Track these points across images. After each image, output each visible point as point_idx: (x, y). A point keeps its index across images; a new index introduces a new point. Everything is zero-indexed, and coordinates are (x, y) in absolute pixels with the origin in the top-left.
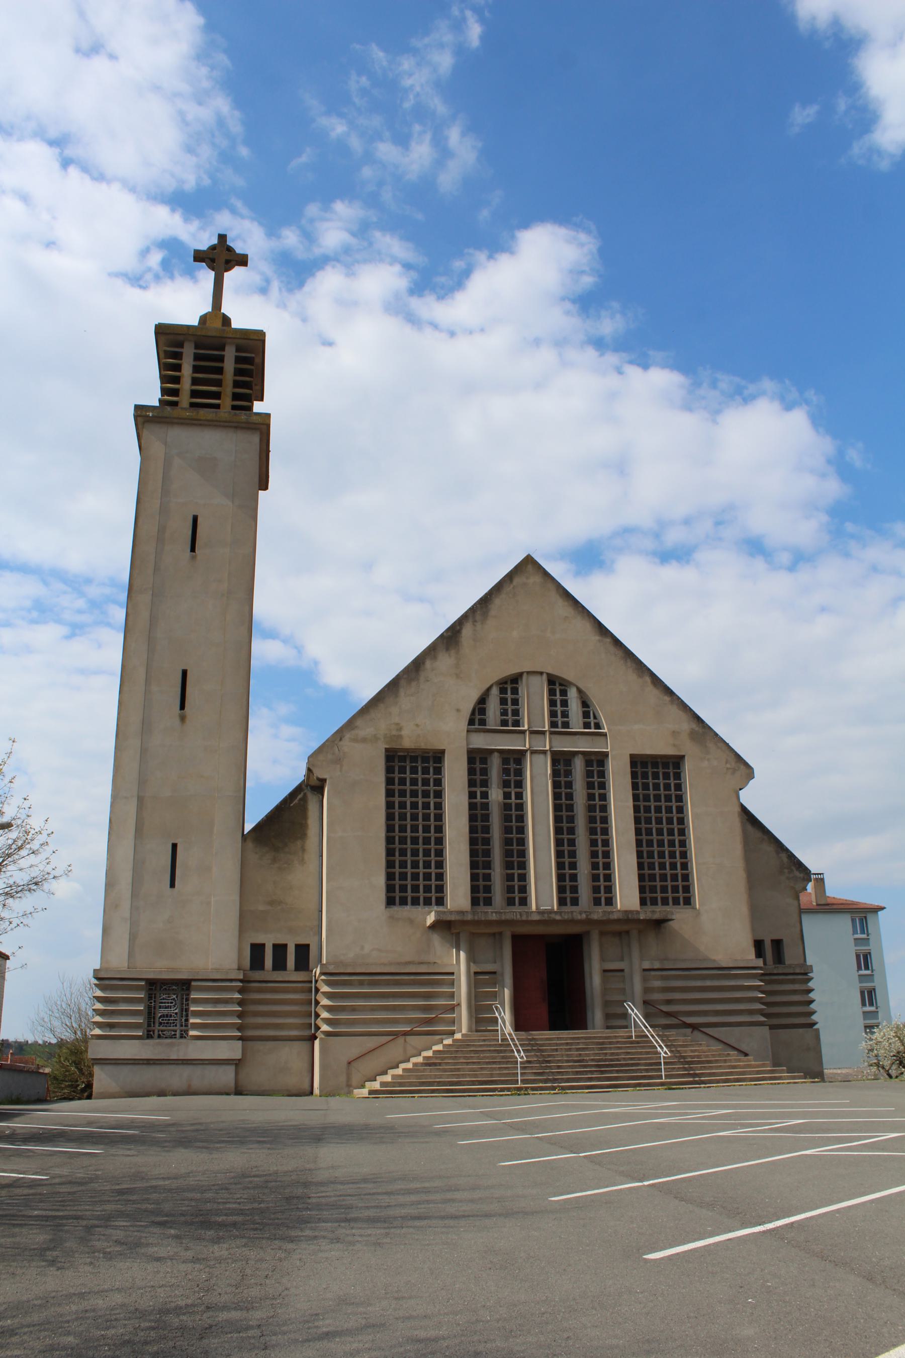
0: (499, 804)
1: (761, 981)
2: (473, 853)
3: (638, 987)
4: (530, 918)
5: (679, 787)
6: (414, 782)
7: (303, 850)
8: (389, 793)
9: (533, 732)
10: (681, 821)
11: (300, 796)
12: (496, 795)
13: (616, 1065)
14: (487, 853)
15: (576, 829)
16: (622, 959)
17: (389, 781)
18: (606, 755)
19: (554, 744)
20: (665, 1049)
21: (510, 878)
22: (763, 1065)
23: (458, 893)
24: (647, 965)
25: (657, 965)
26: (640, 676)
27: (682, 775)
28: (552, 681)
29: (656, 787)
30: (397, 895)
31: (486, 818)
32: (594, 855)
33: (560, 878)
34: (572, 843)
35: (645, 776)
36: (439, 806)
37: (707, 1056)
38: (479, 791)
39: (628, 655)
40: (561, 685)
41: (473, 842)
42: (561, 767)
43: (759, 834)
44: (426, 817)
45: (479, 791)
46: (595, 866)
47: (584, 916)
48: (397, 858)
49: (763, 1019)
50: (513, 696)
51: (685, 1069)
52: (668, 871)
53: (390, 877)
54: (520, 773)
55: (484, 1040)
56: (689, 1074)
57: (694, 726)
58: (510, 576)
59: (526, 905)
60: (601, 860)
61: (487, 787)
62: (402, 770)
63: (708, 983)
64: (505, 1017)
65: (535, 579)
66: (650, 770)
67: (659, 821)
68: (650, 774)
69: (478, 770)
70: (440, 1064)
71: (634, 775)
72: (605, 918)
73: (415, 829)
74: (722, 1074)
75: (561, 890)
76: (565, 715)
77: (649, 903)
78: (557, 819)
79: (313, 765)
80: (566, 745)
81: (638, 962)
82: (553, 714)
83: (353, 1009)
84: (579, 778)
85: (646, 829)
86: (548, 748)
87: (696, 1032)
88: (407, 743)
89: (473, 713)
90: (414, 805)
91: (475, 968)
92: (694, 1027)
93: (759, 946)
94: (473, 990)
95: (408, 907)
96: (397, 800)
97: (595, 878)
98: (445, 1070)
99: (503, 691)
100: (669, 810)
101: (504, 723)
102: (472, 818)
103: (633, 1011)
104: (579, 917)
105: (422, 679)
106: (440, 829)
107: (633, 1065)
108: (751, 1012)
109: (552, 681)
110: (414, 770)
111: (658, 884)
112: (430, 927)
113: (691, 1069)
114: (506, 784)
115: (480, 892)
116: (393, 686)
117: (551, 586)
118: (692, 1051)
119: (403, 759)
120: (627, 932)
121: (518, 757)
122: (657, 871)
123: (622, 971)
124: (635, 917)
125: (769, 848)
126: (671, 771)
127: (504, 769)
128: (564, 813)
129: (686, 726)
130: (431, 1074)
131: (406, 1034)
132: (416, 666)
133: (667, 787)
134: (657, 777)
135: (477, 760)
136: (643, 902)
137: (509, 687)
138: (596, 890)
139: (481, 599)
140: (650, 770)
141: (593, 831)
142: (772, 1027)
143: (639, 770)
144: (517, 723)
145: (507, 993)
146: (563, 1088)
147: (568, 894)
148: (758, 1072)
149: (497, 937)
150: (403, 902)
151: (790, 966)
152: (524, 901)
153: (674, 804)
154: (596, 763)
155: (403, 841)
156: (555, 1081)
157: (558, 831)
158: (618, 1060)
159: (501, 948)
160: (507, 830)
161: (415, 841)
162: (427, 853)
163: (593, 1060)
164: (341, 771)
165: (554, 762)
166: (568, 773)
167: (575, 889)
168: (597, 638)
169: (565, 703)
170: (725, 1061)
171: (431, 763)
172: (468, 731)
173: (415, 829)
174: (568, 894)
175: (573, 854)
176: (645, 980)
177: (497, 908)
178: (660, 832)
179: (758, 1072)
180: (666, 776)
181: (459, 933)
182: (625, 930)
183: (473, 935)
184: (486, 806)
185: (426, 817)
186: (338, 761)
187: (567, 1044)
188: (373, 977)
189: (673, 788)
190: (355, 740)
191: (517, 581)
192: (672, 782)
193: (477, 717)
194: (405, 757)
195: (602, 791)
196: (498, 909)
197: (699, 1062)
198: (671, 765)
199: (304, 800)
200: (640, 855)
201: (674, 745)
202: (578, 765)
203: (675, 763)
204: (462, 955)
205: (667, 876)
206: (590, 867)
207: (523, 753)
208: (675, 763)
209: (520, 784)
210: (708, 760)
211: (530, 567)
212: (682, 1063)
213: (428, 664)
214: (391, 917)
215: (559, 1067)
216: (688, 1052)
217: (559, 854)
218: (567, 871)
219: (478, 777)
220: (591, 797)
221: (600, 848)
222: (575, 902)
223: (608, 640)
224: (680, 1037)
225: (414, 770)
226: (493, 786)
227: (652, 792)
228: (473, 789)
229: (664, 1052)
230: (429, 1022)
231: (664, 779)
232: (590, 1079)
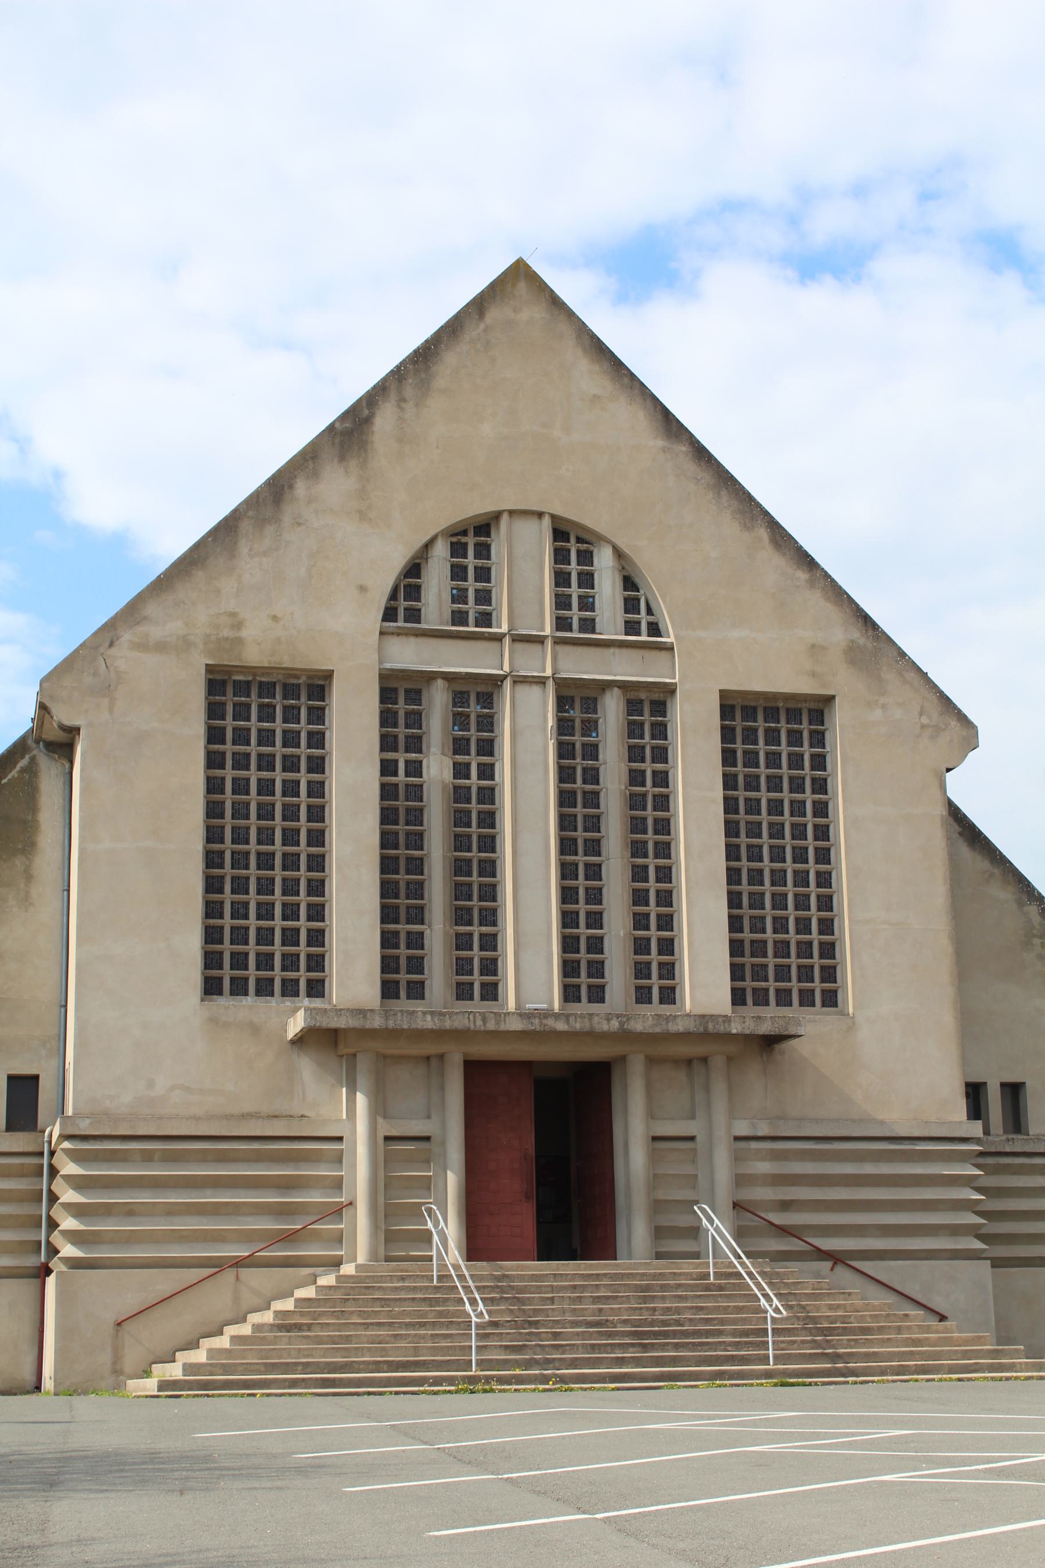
0: (444, 787)
1: (978, 1166)
2: (387, 889)
3: (723, 1168)
4: (503, 1027)
5: (819, 762)
6: (266, 738)
7: (28, 876)
8: (214, 761)
9: (519, 639)
10: (823, 833)
11: (23, 763)
12: (437, 768)
13: (674, 1334)
14: (417, 890)
15: (603, 843)
16: (692, 1117)
17: (214, 735)
18: (670, 690)
19: (562, 665)
20: (776, 1301)
21: (463, 942)
22: (978, 1340)
23: (353, 971)
24: (742, 1128)
25: (764, 1130)
26: (747, 528)
27: (827, 735)
28: (562, 532)
29: (773, 760)
30: (227, 973)
31: (416, 816)
32: (639, 897)
33: (569, 944)
34: (594, 872)
35: (750, 736)
36: (318, 790)
37: (862, 1319)
38: (401, 758)
39: (725, 480)
40: (579, 540)
41: (387, 865)
42: (576, 714)
43: (985, 865)
44: (291, 813)
45: (401, 758)
46: (640, 921)
47: (615, 1024)
48: (228, 897)
49: (979, 1245)
50: (480, 562)
51: (816, 1344)
52: (792, 936)
53: (212, 935)
54: (488, 723)
55: (403, 1279)
56: (825, 1356)
57: (856, 633)
58: (479, 305)
59: (496, 999)
60: (653, 909)
61: (420, 751)
62: (242, 712)
63: (869, 1169)
64: (447, 1229)
65: (533, 313)
66: (761, 725)
67: (777, 831)
68: (761, 734)
69: (401, 715)
70: (309, 1327)
71: (727, 734)
72: (658, 1030)
73: (266, 836)
74: (891, 1356)
75: (569, 969)
76: (587, 604)
77: (749, 1000)
78: (565, 822)
79: (52, 697)
80: (584, 666)
82: (562, 602)
83: (130, 1211)
84: (611, 734)
85: (749, 847)
86: (549, 672)
87: (840, 1269)
88: (254, 656)
89: (394, 596)
90: (266, 787)
91: (386, 1128)
92: (836, 1258)
93: (975, 1093)
94: (381, 1173)
95: (250, 1000)
96: (229, 774)
97: (641, 946)
98: (319, 1340)
99: (458, 550)
100: (798, 808)
101: (459, 618)
102: (387, 816)
104: (605, 1027)
105: (287, 519)
106: (318, 838)
107: (708, 1333)
108: (955, 1230)
109: (562, 532)
110: (267, 713)
111: (771, 961)
112: (293, 1042)
114: (460, 746)
115: (400, 970)
116: (226, 531)
117: (564, 327)
118: (831, 1307)
119: (242, 688)
120: (705, 1060)
121: (486, 690)
122: (769, 935)
123: (692, 1139)
124: (722, 1029)
125: (1004, 894)
126: (805, 727)
127: (456, 715)
128: (579, 810)
129: (840, 633)
130: (290, 1348)
131: (238, 1263)
132: (277, 490)
133: (796, 761)
134: (777, 741)
135: (400, 697)
137: (471, 541)
138: (641, 971)
139: (416, 352)
140: (761, 725)
141: (637, 849)
142: (997, 1263)
143: (739, 723)
144: (485, 619)
145: (453, 1182)
146: (563, 1380)
147: (583, 980)
148: (965, 1355)
149: (432, 1063)
150: (239, 988)
151: (1038, 1138)
152: (491, 992)
153: (809, 797)
154: (650, 706)
155: (240, 860)
156: (547, 1363)
157: (566, 846)
158: (678, 1323)
159: (442, 1088)
160: (460, 842)
161: (266, 861)
162: (291, 887)
163: (625, 1322)
164: (111, 711)
165: (563, 702)
166: (590, 726)
167: (597, 969)
168: (660, 443)
169: (587, 580)
170: (899, 1330)
171: (303, 698)
172: (381, 633)
173: (266, 836)
174: (583, 980)
175: (595, 896)
176: (737, 1158)
177: (437, 1004)
178: (777, 854)
179: (965, 1355)
180: (795, 738)
181: (355, 1055)
182: (697, 1054)
183: (384, 1059)
184: (416, 792)
185: (291, 813)
186: (107, 690)
187: (575, 1287)
188: (171, 1144)
189: (807, 763)
190: (143, 646)
191: (494, 314)
192: (807, 750)
193: (402, 604)
194: (248, 683)
195: (659, 766)
196: (437, 1004)
197: (845, 1331)
198: (806, 716)
199: (32, 770)
200: (734, 900)
201: (814, 674)
202: (612, 712)
203: (812, 712)
204: (361, 1100)
205: (789, 948)
206: (629, 922)
207: (496, 681)
208: (812, 712)
209: (487, 747)
210: (884, 707)
211: (522, 286)
213: (301, 487)
214: (213, 1020)
215: (556, 1336)
216: (822, 1310)
217: (567, 895)
218: (583, 931)
219: (401, 731)
220: (636, 778)
221: (652, 885)
222: (597, 994)
223: (684, 448)
224: (807, 1275)
225: (267, 713)
226: (433, 749)
227: (763, 771)
228: (391, 755)
229: (773, 1308)
230: (288, 1238)
231: (790, 744)
232: (621, 1362)
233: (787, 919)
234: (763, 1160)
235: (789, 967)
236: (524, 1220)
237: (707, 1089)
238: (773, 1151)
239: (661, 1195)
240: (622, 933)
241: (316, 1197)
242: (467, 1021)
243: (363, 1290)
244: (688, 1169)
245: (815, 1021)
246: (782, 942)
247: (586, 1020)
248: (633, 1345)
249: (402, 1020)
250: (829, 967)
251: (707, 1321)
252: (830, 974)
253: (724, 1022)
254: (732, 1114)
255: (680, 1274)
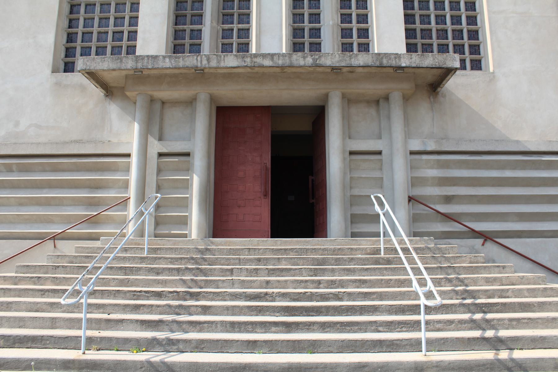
3: (399, 171)
13: (327, 311)
16: (380, 137)
24: (416, 145)
25: (431, 146)
51: (474, 325)
63: (508, 174)
81: (399, 138)
87: (489, 244)
91: (155, 147)
92: (486, 237)
103: (381, 205)
104: (302, 63)
113: (489, 324)
120: (387, 98)
123: (380, 153)
124: (394, 63)
131: (54, 238)
136: (411, 48)
187: (259, 260)
212: (469, 308)
214: (58, 84)
230: (91, 221)
233: (445, 16)
234: (432, 168)
235: (448, 45)
236: (263, 211)
237: (389, 118)
238: (438, 161)
239: (356, 192)
240: (331, 23)
241: (111, 194)
242: (195, 61)
243: (83, 259)
244: (377, 174)
245: (466, 75)
246: (442, 30)
247: (287, 58)
248: (276, 324)
249: (148, 62)
250: (475, 46)
251: (366, 296)
252: (475, 49)
253: (395, 58)
254: (408, 135)
255: (356, 250)
